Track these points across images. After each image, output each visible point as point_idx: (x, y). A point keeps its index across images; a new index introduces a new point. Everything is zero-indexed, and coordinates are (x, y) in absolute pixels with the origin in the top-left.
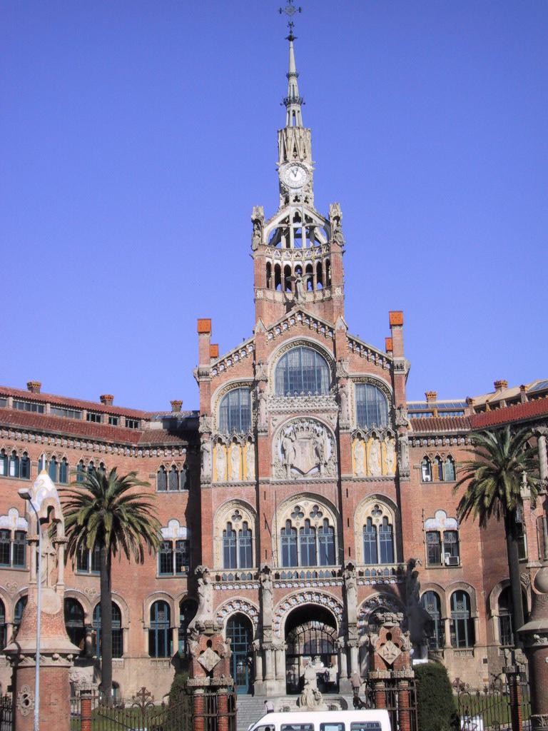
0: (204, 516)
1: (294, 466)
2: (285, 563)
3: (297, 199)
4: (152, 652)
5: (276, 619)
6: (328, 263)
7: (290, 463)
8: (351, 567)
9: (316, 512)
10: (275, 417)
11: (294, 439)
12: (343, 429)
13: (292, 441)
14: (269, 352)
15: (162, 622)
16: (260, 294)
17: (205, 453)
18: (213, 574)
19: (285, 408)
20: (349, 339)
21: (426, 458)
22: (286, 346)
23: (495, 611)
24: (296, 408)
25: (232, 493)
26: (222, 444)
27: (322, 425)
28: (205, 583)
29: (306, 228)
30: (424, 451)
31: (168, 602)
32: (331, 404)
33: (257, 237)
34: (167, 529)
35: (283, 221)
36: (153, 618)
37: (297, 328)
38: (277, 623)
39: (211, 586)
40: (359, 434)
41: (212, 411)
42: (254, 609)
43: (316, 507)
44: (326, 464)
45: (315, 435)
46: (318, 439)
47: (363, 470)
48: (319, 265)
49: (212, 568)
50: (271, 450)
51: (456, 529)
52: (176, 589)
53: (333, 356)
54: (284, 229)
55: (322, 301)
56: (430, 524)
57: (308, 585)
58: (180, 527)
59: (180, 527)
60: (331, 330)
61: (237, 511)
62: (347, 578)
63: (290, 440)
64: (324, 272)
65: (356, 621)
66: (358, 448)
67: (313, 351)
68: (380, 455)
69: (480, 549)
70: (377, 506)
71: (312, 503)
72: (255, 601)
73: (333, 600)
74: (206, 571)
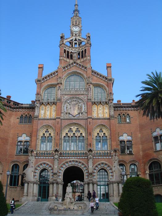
1: (70, 113)
3: (76, 35)
4: (11, 184)
5: (59, 171)
6: (85, 50)
8: (91, 151)
9: (78, 130)
10: (64, 96)
11: (70, 104)
12: (89, 100)
13: (70, 105)
15: (16, 172)
16: (61, 58)
17: (36, 107)
18: (35, 152)
20: (92, 71)
21: (119, 114)
22: (69, 74)
23: (148, 172)
25: (45, 123)
26: (44, 105)
27: (81, 100)
28: (32, 156)
30: (118, 112)
31: (19, 164)
32: (85, 92)
35: (71, 40)
36: (12, 170)
37: (73, 68)
38: (60, 173)
39: (34, 157)
40: (95, 103)
41: (41, 93)
42: (50, 166)
43: (78, 129)
44: (82, 113)
45: (78, 103)
46: (79, 104)
47: (96, 115)
48: (82, 51)
49: (36, 150)
50: (61, 107)
51: (131, 140)
52: (22, 160)
54: (72, 43)
55: (83, 61)
56: (121, 138)
57: (74, 158)
58: (26, 136)
59: (26, 136)
60: (86, 68)
61: (47, 130)
62: (89, 155)
63: (69, 105)
64: (84, 53)
66: (95, 108)
67: (79, 76)
69: (140, 148)
70: (101, 129)
71: (76, 127)
72: (51, 164)
73: (83, 164)
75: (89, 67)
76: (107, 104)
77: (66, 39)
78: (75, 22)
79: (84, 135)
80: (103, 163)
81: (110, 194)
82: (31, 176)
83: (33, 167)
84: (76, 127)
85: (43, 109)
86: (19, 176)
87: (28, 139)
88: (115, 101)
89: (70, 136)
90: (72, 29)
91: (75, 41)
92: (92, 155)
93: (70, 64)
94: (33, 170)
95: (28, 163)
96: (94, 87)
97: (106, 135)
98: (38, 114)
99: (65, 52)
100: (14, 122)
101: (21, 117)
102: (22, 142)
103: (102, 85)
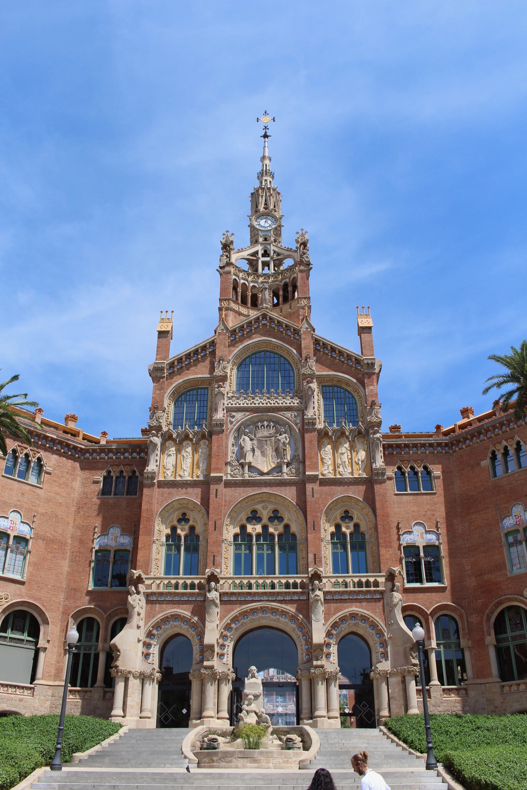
0: (144, 514)
2: (237, 571)
3: (266, 239)
6: (294, 281)
7: (247, 461)
8: (317, 576)
9: (276, 517)
14: (230, 352)
19: (245, 405)
23: (491, 639)
24: (257, 405)
28: (138, 593)
29: (274, 261)
33: (225, 257)
34: (106, 537)
41: (166, 405)
43: (275, 511)
48: (286, 286)
50: (227, 447)
51: (437, 544)
53: (299, 356)
60: (296, 332)
61: (184, 514)
64: (290, 289)
65: (322, 641)
68: (349, 454)
70: (346, 512)
74: (139, 577)
75: (307, 328)
76: (364, 437)
77: (239, 251)
78: (263, 205)
79: (294, 529)
80: (353, 616)
81: (379, 711)
82: (137, 655)
83: (142, 627)
84: (271, 507)
85: (170, 453)
86: (97, 657)
87: (126, 541)
88: (385, 429)
89: (254, 534)
90: (255, 224)
91: (263, 256)
92: (319, 590)
93: (250, 322)
94: (143, 638)
95: (124, 616)
96: (323, 386)
97: (363, 528)
98: (156, 469)
99: (235, 288)
100: (84, 493)
101: (105, 478)
102: (110, 551)
103: (348, 383)
